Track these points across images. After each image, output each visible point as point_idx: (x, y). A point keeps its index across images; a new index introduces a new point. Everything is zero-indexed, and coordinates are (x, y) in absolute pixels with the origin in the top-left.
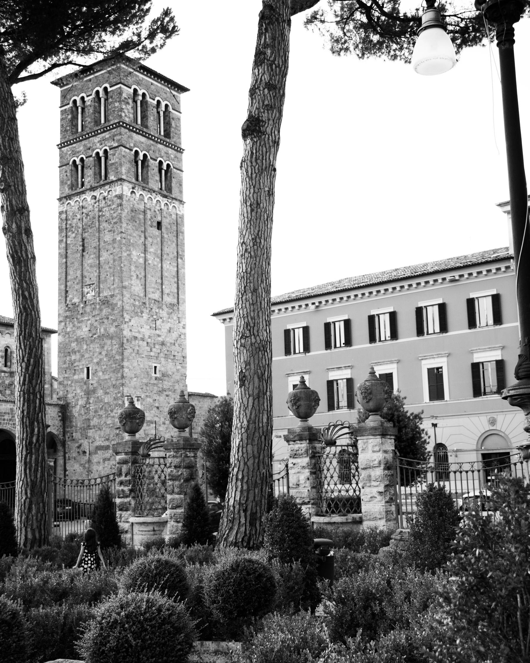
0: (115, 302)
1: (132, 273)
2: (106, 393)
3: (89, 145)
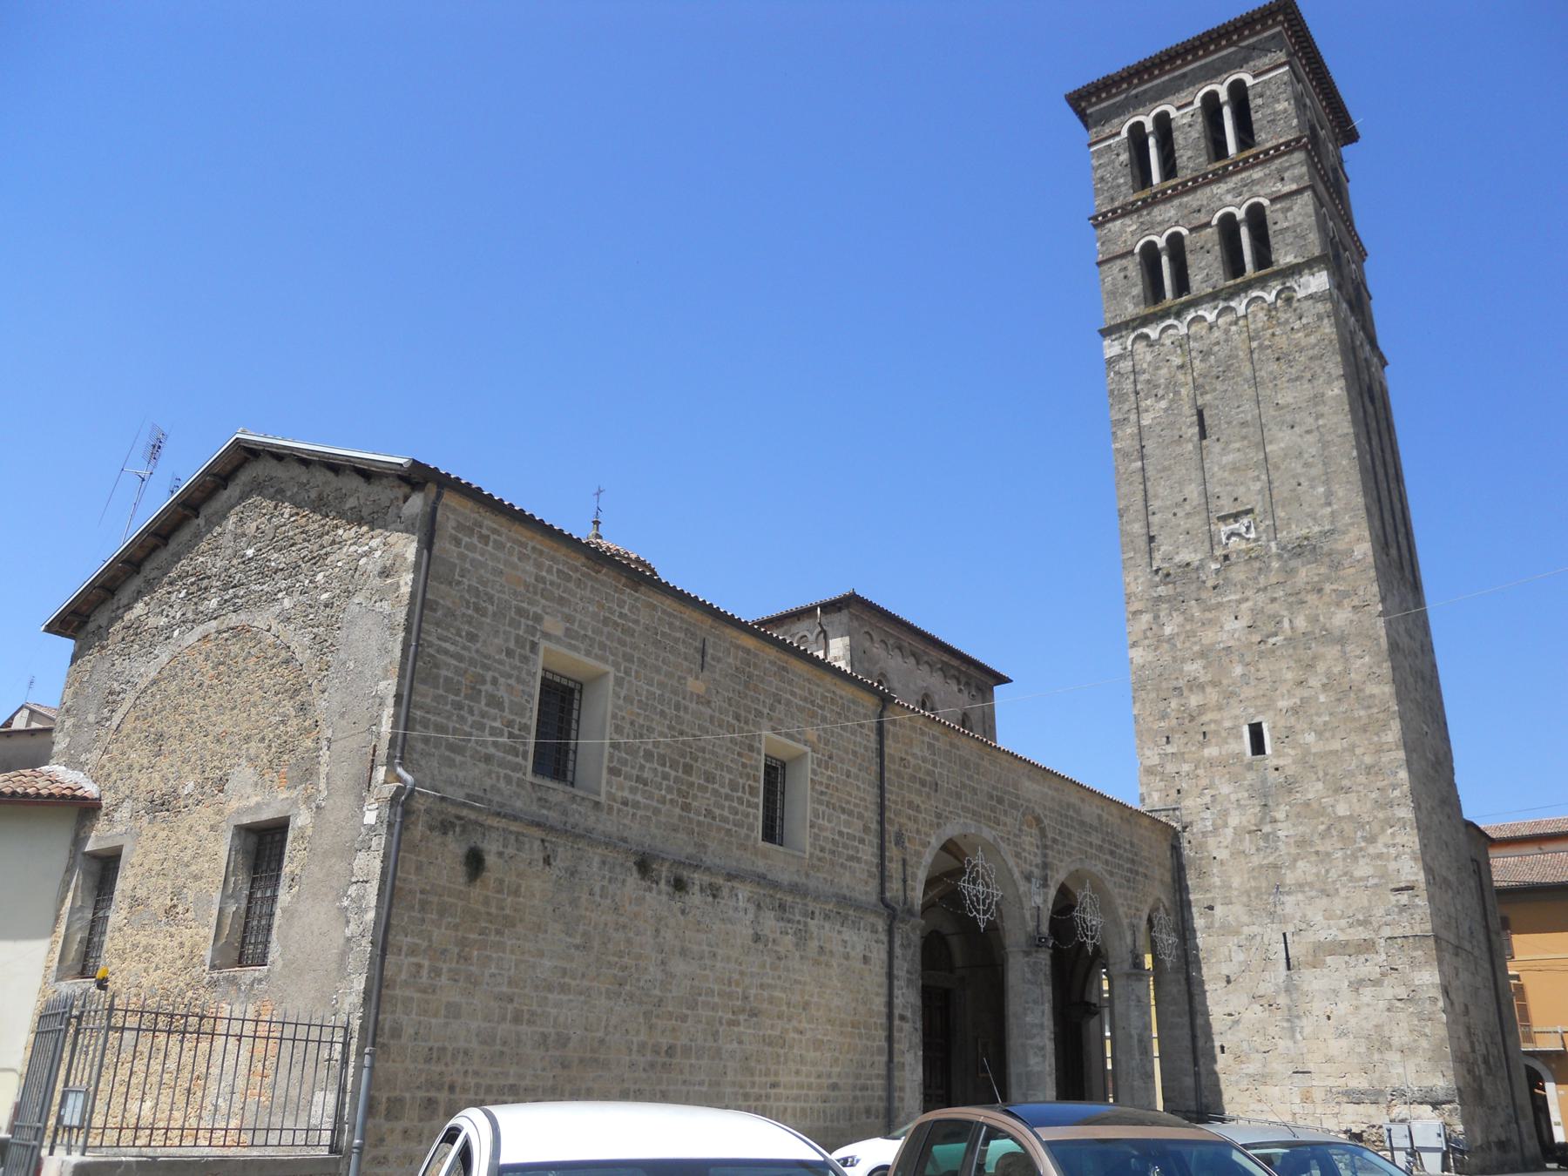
0: (1341, 546)
2: (1339, 790)
3: (1195, 205)
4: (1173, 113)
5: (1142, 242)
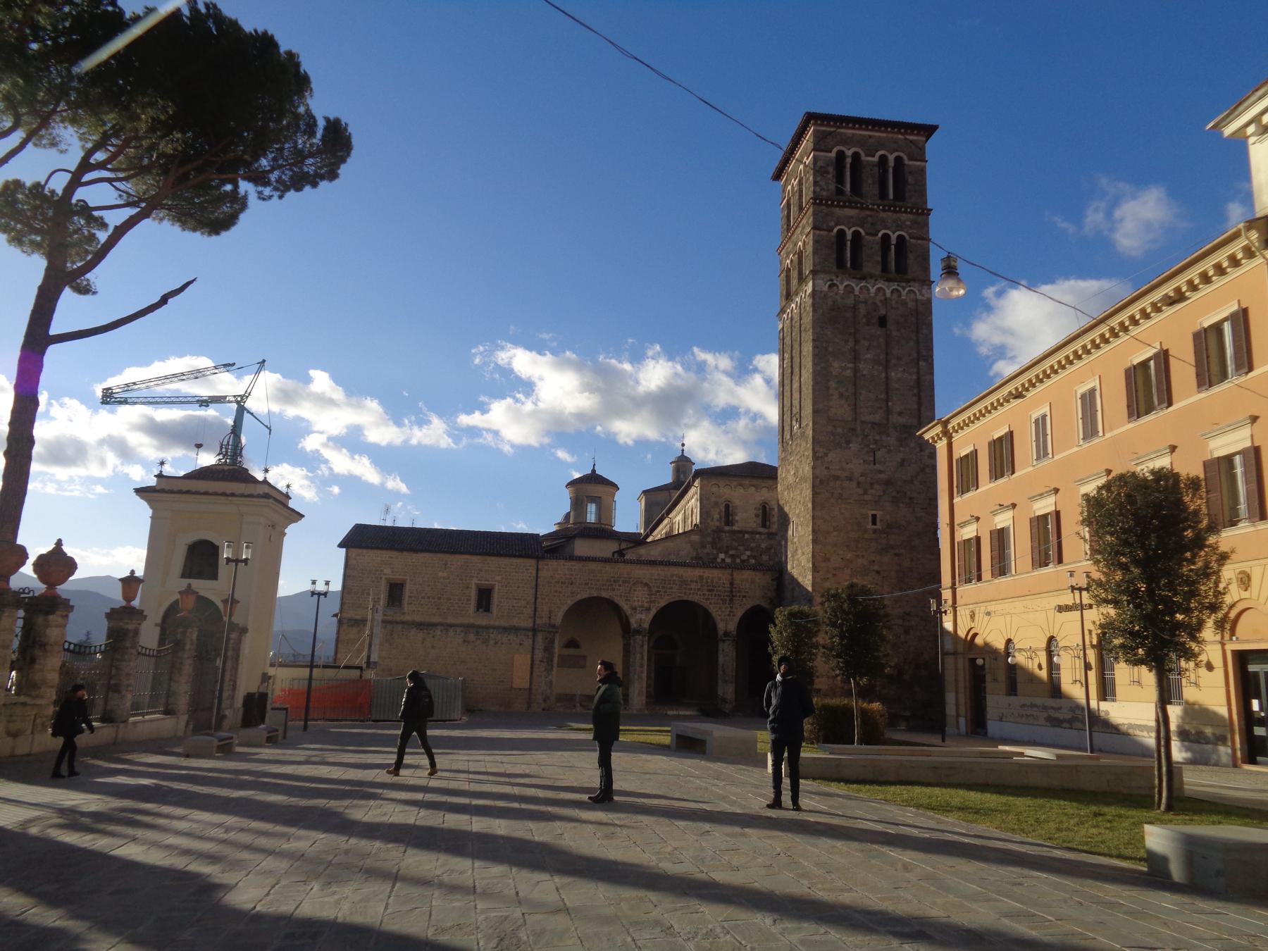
1: (831, 391)
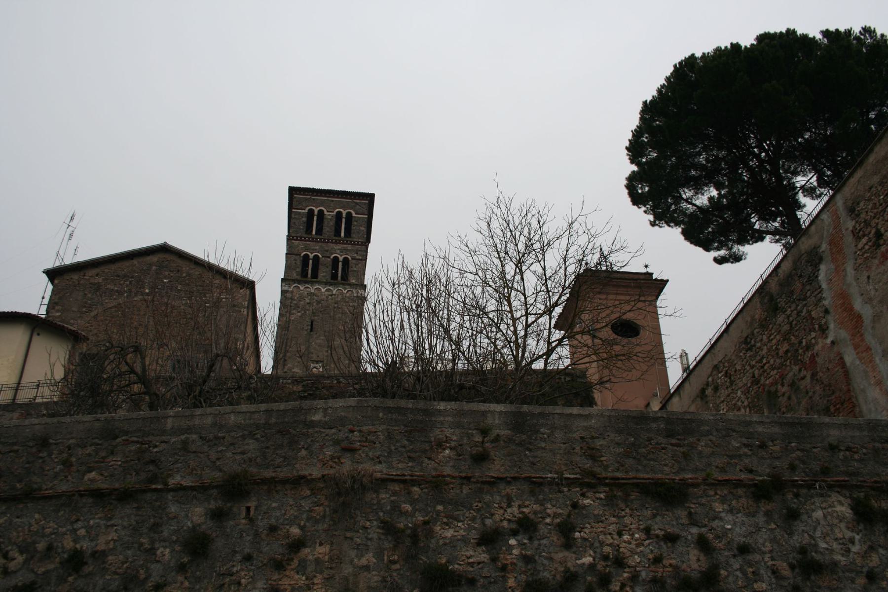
3: (326, 248)
4: (326, 212)
5: (304, 253)
